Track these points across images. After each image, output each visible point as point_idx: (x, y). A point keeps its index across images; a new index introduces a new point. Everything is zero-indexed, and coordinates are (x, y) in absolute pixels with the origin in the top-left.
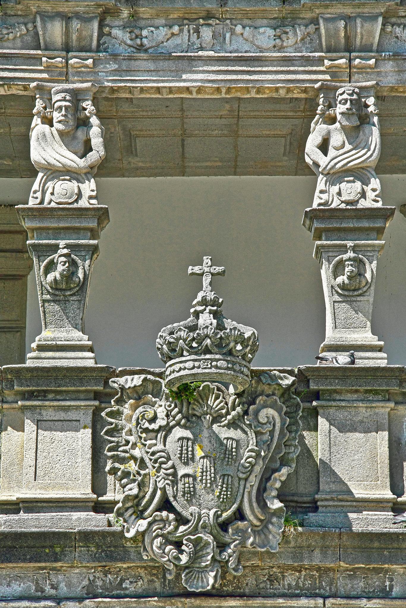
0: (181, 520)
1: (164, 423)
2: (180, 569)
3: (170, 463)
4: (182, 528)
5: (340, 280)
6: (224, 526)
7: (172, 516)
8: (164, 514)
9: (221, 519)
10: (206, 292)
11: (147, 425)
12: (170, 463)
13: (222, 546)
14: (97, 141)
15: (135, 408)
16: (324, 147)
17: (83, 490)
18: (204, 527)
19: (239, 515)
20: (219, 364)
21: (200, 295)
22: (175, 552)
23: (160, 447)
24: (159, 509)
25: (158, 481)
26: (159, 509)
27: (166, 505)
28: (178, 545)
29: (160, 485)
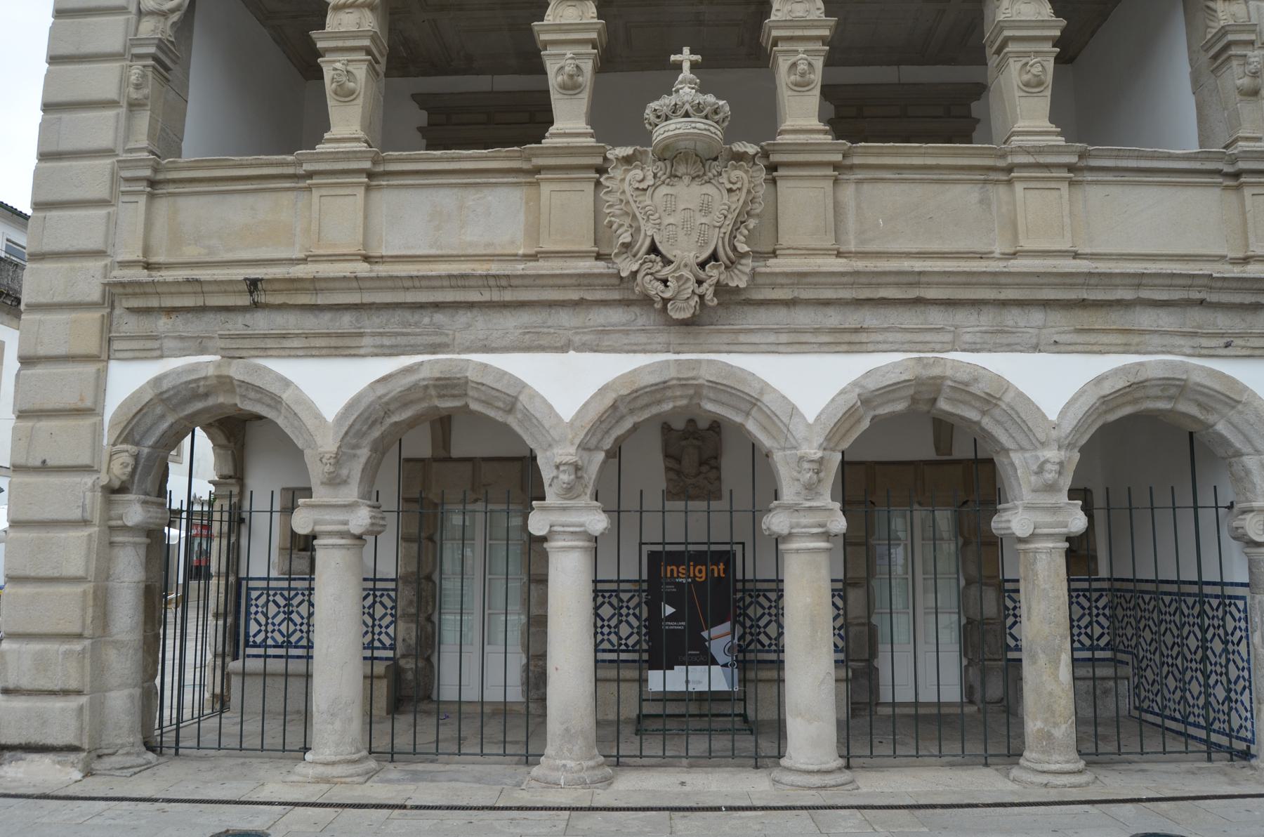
0: (667, 262)
1: (651, 183)
2: (665, 301)
3: (657, 215)
4: (668, 268)
5: (793, 78)
6: (702, 265)
7: (658, 259)
8: (653, 256)
9: (700, 260)
10: (686, 72)
11: (637, 185)
12: (657, 215)
13: (700, 282)
15: (627, 171)
17: (588, 246)
18: (686, 266)
19: (714, 257)
20: (698, 125)
21: (681, 77)
22: (661, 287)
23: (648, 202)
24: (648, 253)
25: (648, 229)
26: (648, 253)
27: (653, 249)
28: (665, 282)
29: (649, 233)
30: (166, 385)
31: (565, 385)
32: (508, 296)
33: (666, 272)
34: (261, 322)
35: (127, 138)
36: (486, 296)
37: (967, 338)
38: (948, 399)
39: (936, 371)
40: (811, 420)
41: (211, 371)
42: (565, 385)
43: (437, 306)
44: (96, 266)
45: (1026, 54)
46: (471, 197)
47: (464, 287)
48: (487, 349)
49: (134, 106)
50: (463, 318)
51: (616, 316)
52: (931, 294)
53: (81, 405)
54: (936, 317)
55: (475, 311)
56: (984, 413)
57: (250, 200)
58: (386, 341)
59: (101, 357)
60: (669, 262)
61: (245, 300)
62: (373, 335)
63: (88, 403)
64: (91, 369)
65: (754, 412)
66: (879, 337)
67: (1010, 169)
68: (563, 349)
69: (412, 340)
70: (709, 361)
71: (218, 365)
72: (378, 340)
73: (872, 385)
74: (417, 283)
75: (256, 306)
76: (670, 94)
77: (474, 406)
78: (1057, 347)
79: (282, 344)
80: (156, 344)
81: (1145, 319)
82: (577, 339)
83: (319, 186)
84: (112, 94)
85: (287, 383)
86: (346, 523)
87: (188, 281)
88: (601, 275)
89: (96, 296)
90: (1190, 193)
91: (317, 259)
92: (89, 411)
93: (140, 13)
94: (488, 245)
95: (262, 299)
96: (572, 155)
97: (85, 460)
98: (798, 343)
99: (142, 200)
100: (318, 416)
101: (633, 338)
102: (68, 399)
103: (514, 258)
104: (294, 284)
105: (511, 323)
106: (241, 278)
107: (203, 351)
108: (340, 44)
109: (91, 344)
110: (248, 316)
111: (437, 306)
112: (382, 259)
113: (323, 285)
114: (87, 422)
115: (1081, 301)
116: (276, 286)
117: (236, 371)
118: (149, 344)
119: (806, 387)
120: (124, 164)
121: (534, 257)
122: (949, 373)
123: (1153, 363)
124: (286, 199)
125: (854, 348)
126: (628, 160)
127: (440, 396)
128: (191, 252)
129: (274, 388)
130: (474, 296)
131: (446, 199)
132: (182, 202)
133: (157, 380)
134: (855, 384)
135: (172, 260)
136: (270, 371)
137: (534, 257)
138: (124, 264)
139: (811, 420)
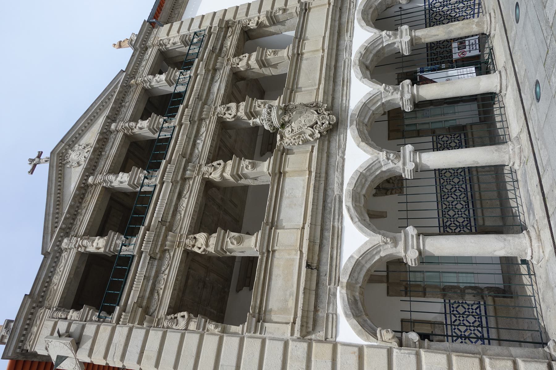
2: (329, 124)
14: (218, 162)
15: (285, 137)
16: (231, 115)
19: (317, 111)
30: (349, 313)
31: (356, 157)
32: (323, 175)
33: (319, 123)
34: (325, 268)
35: (238, 334)
36: (323, 182)
37: (347, 56)
38: (367, 60)
39: (357, 62)
40: (372, 89)
41: (344, 291)
42: (356, 157)
43: (325, 201)
44: (291, 345)
45: (266, 55)
46: (286, 194)
47: (318, 189)
48: (342, 184)
49: (224, 331)
50: (330, 192)
51: (334, 145)
52: (333, 63)
53: (357, 354)
54: (341, 64)
55: (327, 188)
56: (371, 53)
57: (273, 277)
58: (337, 217)
60: (317, 123)
61: (315, 272)
62: (334, 222)
63: (356, 349)
64: (339, 348)
65: (369, 106)
66: (346, 75)
67: (298, 54)
68: (344, 160)
69: (337, 208)
70: (351, 117)
71: (342, 287)
72: (336, 220)
73: (360, 75)
74: (316, 204)
75: (318, 268)
76: (263, 126)
77: (364, 192)
78: (351, 36)
79: (335, 259)
80: (331, 316)
81: (344, 19)
82: (340, 155)
83: (273, 246)
84: (217, 338)
85: (352, 257)
86: (412, 236)
87: (304, 293)
88: (319, 145)
89: (304, 345)
90: (310, 18)
91: (301, 246)
92: (361, 349)
93: (186, 329)
94: (304, 188)
95: (315, 265)
96: (276, 165)
97: (385, 351)
98: (348, 95)
99: (266, 325)
100: (366, 243)
101: (342, 138)
102: (353, 360)
103: (309, 179)
104: (310, 249)
106: (305, 269)
107: (335, 295)
108: (221, 241)
109: (328, 348)
110: (321, 274)
111: (325, 201)
112: (304, 224)
113: (312, 238)
114: (365, 350)
115: (338, 32)
116: (311, 257)
117: (344, 279)
118: (330, 319)
119: (360, 91)
120: (249, 331)
121: (310, 172)
122: (358, 58)
123: (357, 15)
124: (276, 262)
125: (349, 81)
126: (282, 138)
127: (360, 202)
129: (353, 262)
130: (322, 186)
131: (285, 202)
132: (270, 307)
133: (346, 315)
134: (360, 80)
135: (293, 311)
136: (346, 264)
137: (310, 172)
138: (292, 334)
139: (372, 89)
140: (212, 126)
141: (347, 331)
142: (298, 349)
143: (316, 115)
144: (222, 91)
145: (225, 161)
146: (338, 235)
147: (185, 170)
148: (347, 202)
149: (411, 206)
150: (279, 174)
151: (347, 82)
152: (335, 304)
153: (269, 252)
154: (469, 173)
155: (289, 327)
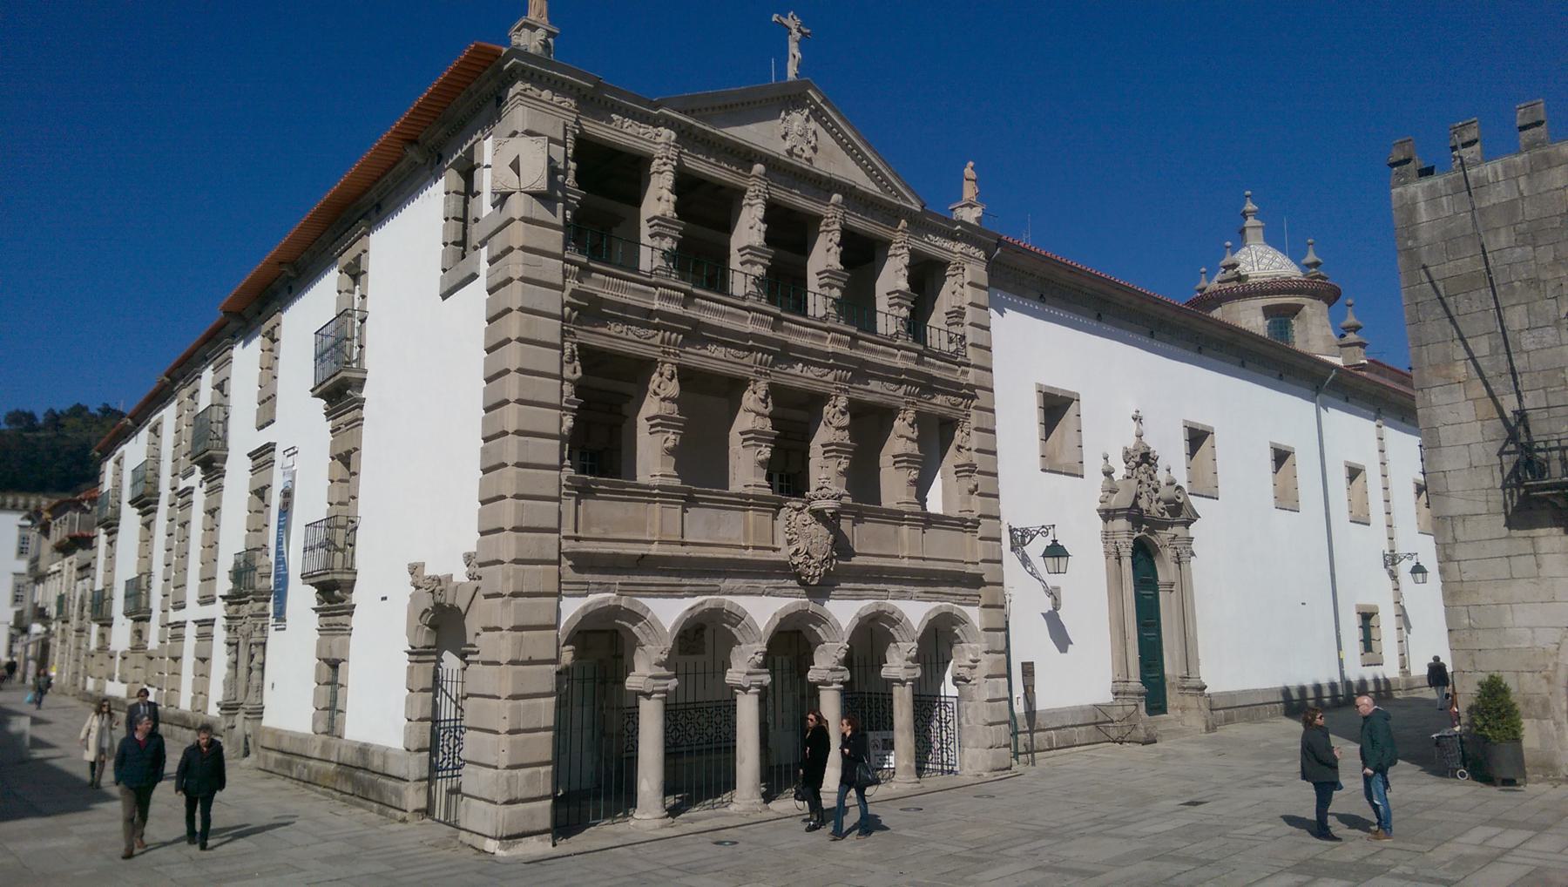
31: (762, 610)
41: (611, 603)
46: (723, 512)
59: (558, 595)
73: (864, 614)
92: (556, 627)
105: (740, 583)
107: (607, 591)
117: (624, 602)
123: (945, 606)
128: (596, 532)
133: (585, 608)
140: (819, 388)
141: (572, 608)
142: (548, 545)
143: (821, 557)
144: (869, 398)
145: (771, 416)
146: (672, 592)
147: (764, 351)
148: (710, 600)
149: (700, 678)
150: (744, 502)
151: (857, 595)
152: (598, 591)
153: (646, 494)
154: (728, 746)
155: (573, 534)
